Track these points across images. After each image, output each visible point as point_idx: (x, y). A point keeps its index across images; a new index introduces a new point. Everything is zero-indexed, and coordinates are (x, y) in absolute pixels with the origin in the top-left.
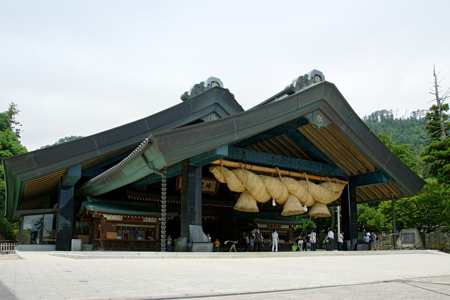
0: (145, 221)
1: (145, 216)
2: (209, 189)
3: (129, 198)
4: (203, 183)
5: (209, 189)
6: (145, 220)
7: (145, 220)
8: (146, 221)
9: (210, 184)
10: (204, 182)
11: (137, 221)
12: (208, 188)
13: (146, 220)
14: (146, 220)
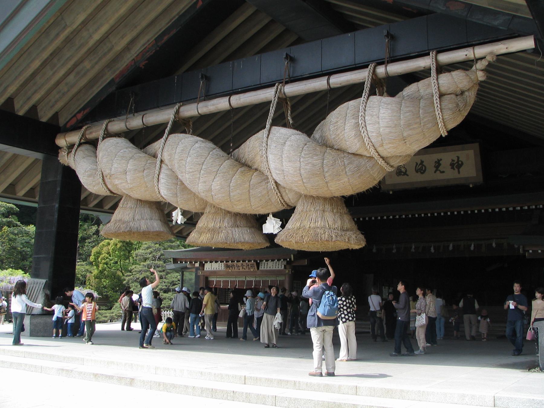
0: (263, 268)
2: (459, 172)
4: (441, 162)
5: (459, 172)
6: (263, 265)
7: (263, 265)
8: (265, 268)
10: (441, 160)
11: (248, 268)
12: (456, 170)
13: (266, 265)
14: (266, 265)
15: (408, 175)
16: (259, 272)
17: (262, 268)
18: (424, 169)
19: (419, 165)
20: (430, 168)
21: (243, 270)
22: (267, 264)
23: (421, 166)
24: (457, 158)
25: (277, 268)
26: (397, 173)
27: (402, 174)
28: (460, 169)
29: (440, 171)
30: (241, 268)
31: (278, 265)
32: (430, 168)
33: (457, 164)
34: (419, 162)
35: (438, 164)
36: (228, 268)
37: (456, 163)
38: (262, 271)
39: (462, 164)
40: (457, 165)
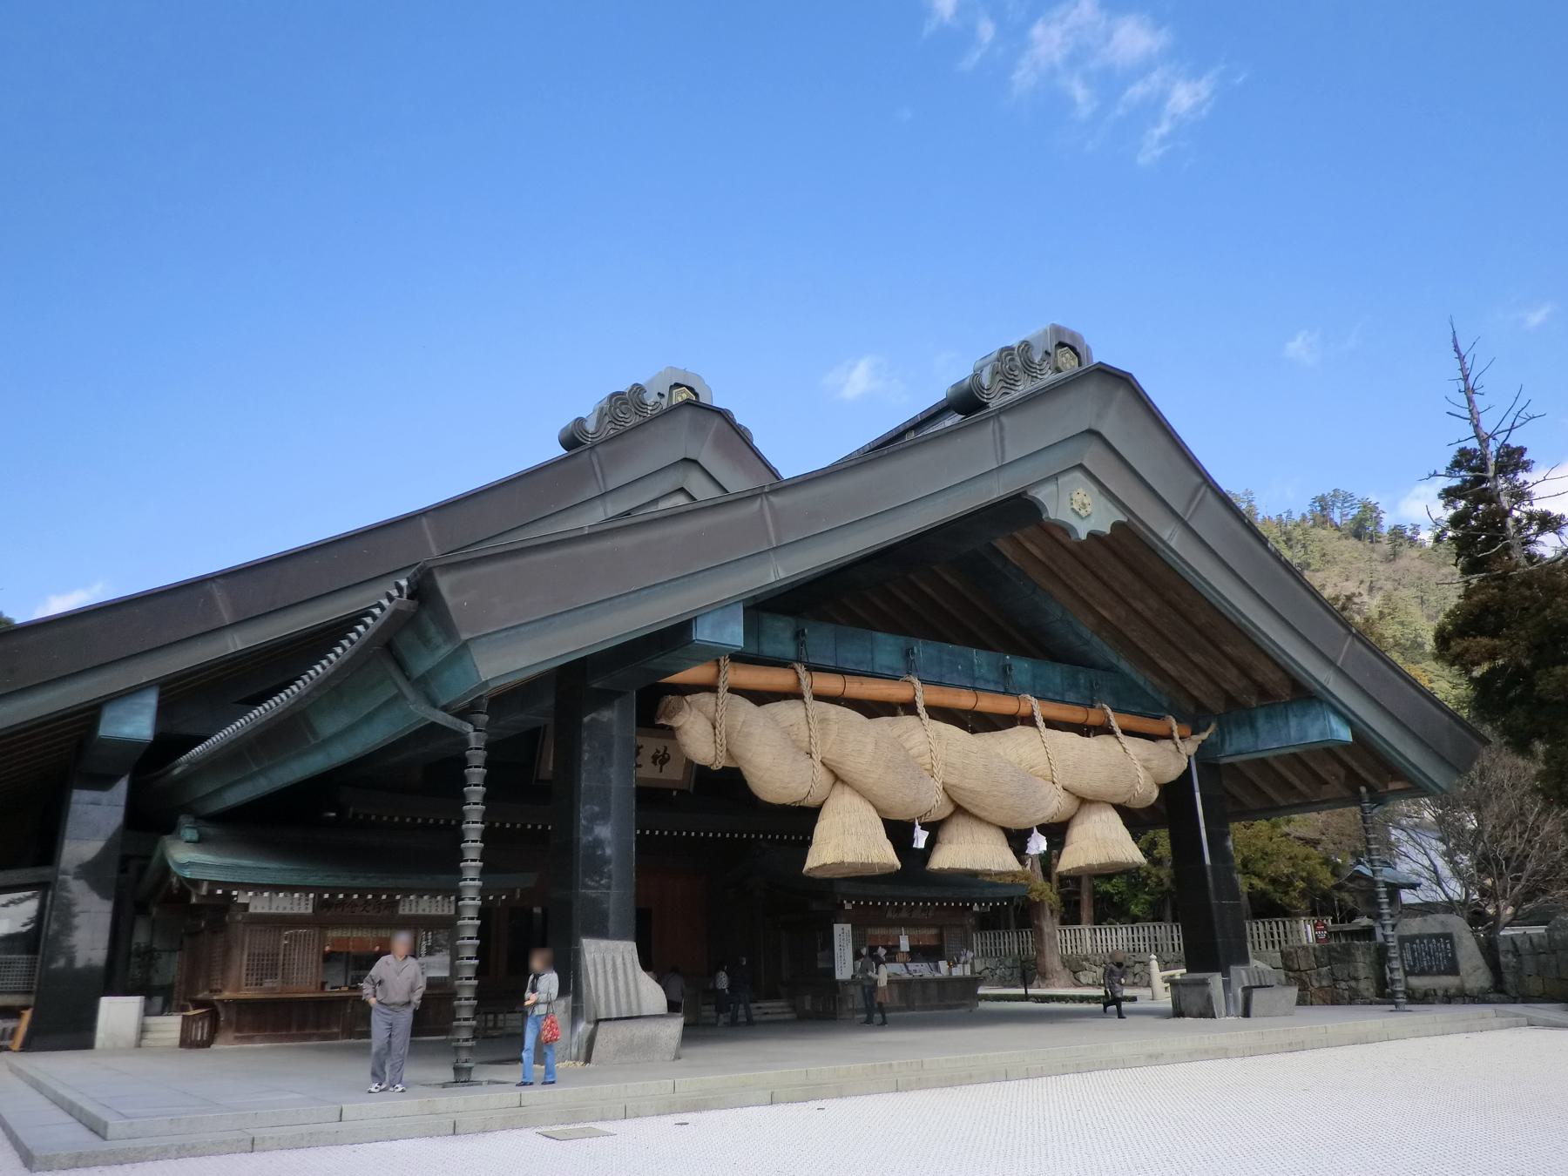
1: (407, 892)
2: (661, 771)
3: (350, 816)
5: (661, 771)
7: (407, 904)
8: (413, 912)
9: (665, 752)
10: (642, 747)
25: (440, 913)
28: (664, 767)
31: (443, 906)
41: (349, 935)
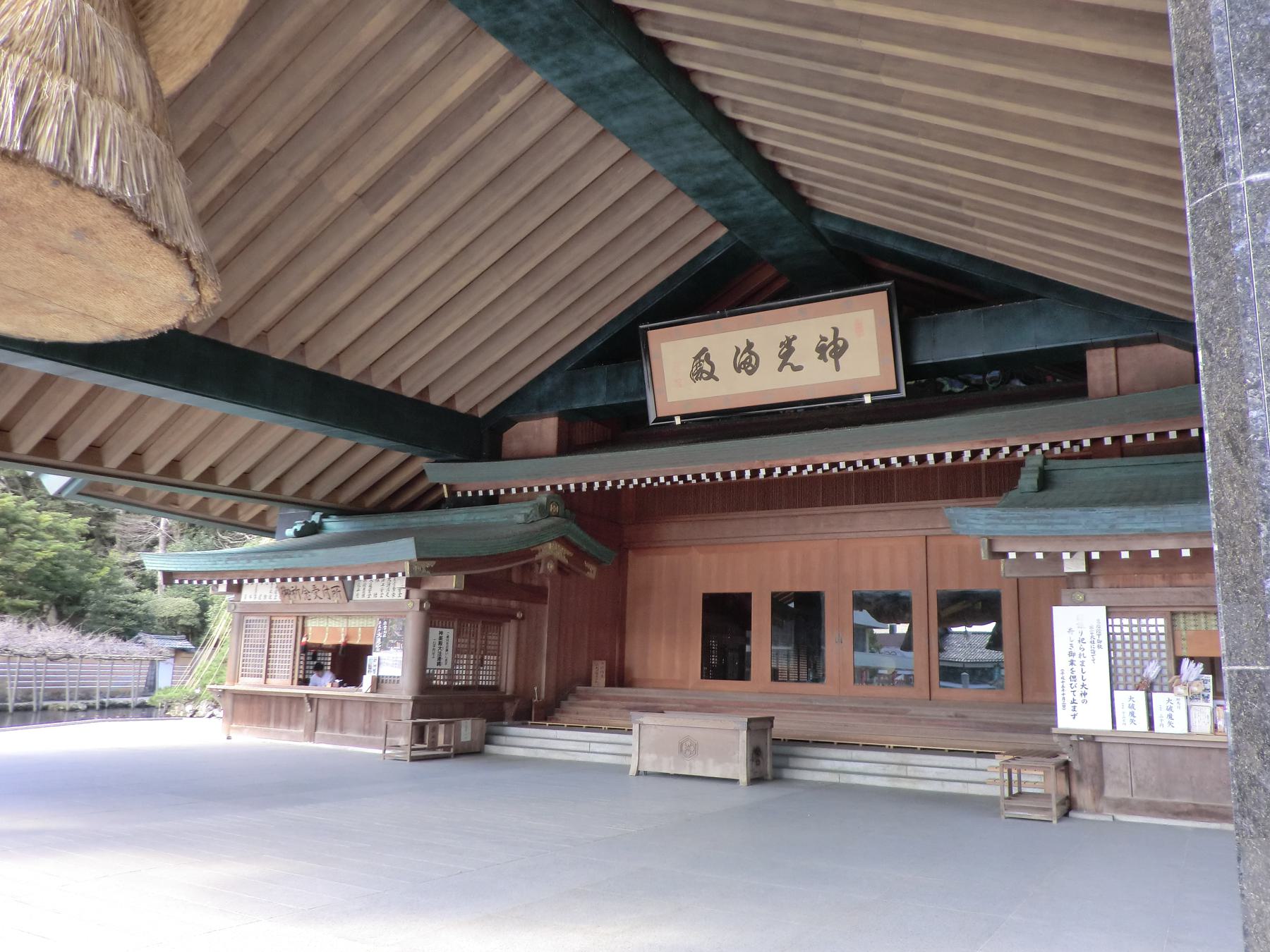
0: (360, 598)
2: (838, 368)
4: (794, 344)
5: (838, 368)
6: (361, 588)
7: (361, 588)
8: (366, 598)
10: (794, 338)
11: (327, 596)
12: (831, 361)
13: (367, 588)
14: (367, 588)
15: (717, 379)
16: (350, 607)
17: (358, 595)
18: (753, 363)
19: (744, 352)
20: (768, 354)
21: (318, 600)
22: (370, 586)
23: (747, 355)
24: (832, 331)
25: (391, 598)
26: (694, 375)
27: (705, 375)
28: (840, 360)
29: (791, 365)
30: (313, 596)
32: (768, 354)
33: (832, 347)
34: (743, 347)
35: (788, 347)
36: (287, 597)
37: (830, 345)
38: (359, 603)
39: (846, 346)
40: (833, 349)
41: (325, 625)
